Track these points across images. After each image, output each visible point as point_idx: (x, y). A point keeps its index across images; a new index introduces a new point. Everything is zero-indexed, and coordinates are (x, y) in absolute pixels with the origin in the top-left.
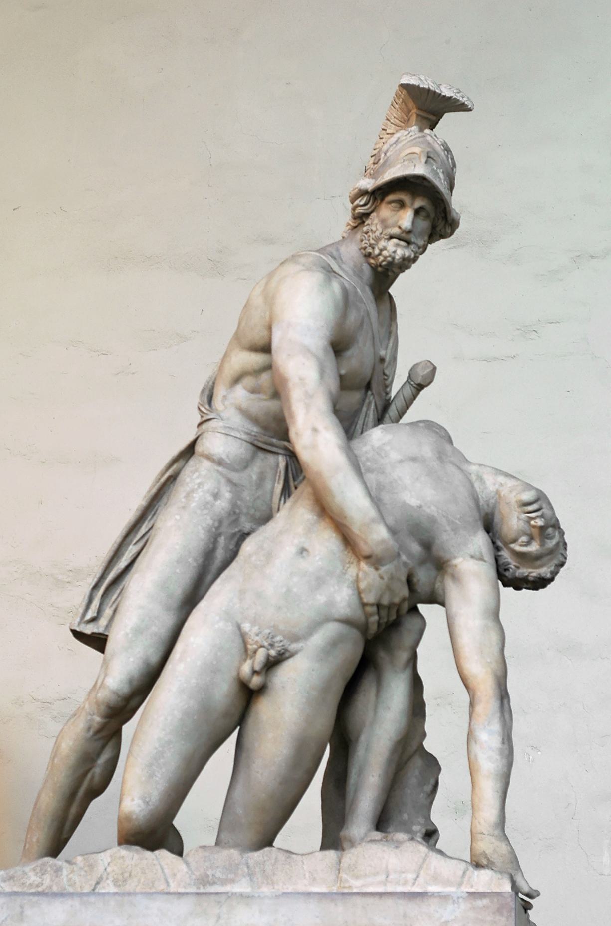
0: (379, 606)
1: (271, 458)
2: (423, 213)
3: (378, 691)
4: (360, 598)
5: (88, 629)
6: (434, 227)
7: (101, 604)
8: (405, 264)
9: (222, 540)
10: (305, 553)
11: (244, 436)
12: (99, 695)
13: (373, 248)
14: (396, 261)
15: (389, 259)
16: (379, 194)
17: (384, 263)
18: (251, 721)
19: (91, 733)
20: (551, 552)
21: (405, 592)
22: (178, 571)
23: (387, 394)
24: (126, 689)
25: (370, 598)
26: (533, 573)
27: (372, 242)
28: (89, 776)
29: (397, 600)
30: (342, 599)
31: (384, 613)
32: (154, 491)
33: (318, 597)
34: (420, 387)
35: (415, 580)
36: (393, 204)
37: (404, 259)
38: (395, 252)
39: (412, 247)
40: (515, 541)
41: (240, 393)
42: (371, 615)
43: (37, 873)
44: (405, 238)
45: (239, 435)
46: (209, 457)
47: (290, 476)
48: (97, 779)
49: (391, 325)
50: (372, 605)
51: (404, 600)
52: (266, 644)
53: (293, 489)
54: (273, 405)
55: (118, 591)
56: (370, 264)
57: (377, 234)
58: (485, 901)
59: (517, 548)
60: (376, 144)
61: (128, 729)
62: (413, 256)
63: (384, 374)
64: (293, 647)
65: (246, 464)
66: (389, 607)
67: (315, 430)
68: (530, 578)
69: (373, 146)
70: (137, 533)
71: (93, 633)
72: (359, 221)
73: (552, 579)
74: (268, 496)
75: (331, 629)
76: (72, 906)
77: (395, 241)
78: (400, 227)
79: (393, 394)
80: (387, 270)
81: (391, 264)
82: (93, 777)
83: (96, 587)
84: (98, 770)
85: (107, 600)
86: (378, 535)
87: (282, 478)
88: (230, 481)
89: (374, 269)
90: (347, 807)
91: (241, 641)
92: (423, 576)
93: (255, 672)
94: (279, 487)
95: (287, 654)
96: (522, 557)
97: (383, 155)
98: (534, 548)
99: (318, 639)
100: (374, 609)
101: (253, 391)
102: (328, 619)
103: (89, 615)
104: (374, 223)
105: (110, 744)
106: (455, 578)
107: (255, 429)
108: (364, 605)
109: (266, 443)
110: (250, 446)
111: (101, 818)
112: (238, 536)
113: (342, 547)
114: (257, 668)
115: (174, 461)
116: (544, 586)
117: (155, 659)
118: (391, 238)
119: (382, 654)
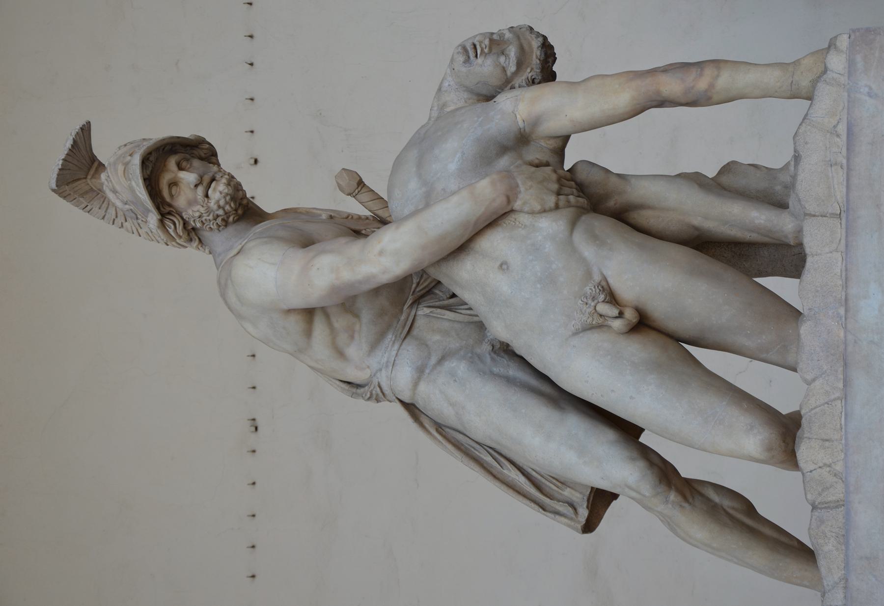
0: (558, 194)
1: (420, 322)
2: (184, 164)
3: (649, 207)
4: (551, 210)
5: (584, 513)
6: (201, 159)
7: (559, 501)
8: (236, 188)
9: (495, 370)
10: (505, 267)
11: (396, 347)
12: (647, 494)
13: (218, 216)
14: (231, 192)
15: (228, 198)
16: (165, 209)
17: (232, 205)
18: (673, 325)
19: (686, 505)
20: (518, 38)
21: (548, 169)
22: (523, 411)
23: (367, 218)
24: (641, 464)
25: (551, 200)
26: (536, 54)
27: (211, 217)
28: (731, 512)
29: (554, 177)
30: (550, 227)
31: (566, 190)
32: (450, 446)
33: (546, 250)
34: (361, 183)
35: (537, 161)
36: (173, 192)
37: (228, 184)
38: (221, 193)
39: (218, 176)
40: (504, 70)
41: (352, 351)
42: (569, 202)
43: (829, 552)
44: (206, 183)
45: (394, 353)
46: (416, 384)
47: (437, 304)
48: (735, 504)
49: (300, 213)
50: (558, 200)
51: (555, 171)
52: (593, 304)
53: (452, 301)
54: (366, 316)
55: (548, 483)
56: (235, 222)
57: (202, 210)
58: (859, 58)
59: (512, 68)
60: (128, 231)
61: (686, 471)
62: (226, 176)
63: (347, 218)
64: (597, 278)
65: (423, 344)
66: (562, 186)
67: (381, 253)
68: (543, 56)
69: (131, 234)
70: (492, 466)
71: (587, 507)
72: (193, 234)
73: (545, 38)
74: (456, 325)
75: (578, 237)
76: (859, 503)
77: (210, 192)
78: (196, 186)
79: (368, 213)
80: (240, 204)
81: (233, 199)
82: (733, 508)
83: (543, 508)
84: (726, 503)
85: (556, 495)
86: (487, 191)
87: (439, 310)
88: (441, 360)
89: (239, 219)
90: (766, 239)
91: (589, 332)
92: (533, 154)
93: (621, 315)
94: (449, 315)
95: (604, 284)
96: (520, 65)
97: (127, 206)
98: (512, 52)
99: (588, 251)
100: (561, 197)
101: (352, 337)
103: (568, 511)
104: (192, 213)
105: (700, 488)
106: (536, 122)
107: (390, 336)
108: (557, 207)
109: (404, 327)
110: (406, 340)
111: (777, 497)
112: (495, 356)
113: (499, 229)
114: (615, 312)
115: (422, 425)
116: (552, 47)
117: (609, 435)
118: (207, 196)
119: (611, 203)
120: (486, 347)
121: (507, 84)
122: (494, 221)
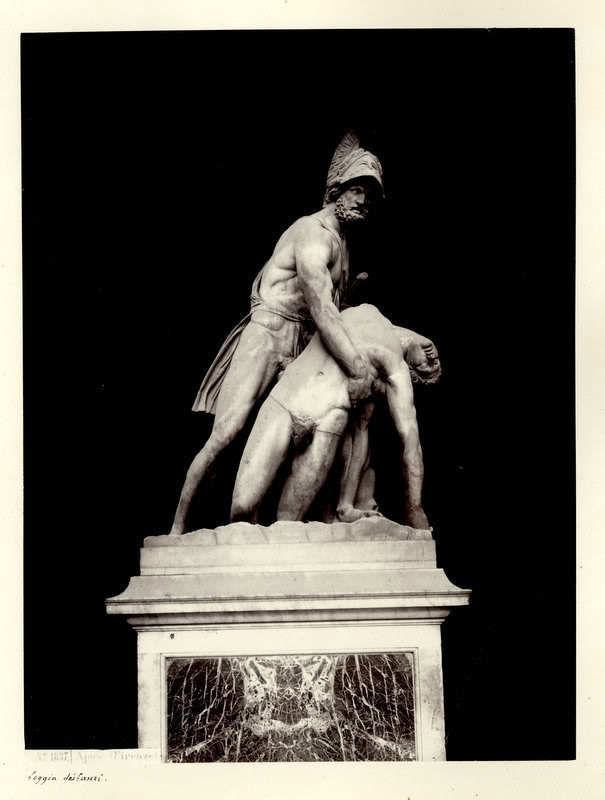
1: (291, 326)
3: (353, 440)
9: (270, 365)
25: (354, 397)
40: (420, 365)
88: (273, 336)
98: (429, 369)
102: (335, 407)
108: (351, 399)
120: (281, 358)
121: (413, 366)
122: (346, 371)
